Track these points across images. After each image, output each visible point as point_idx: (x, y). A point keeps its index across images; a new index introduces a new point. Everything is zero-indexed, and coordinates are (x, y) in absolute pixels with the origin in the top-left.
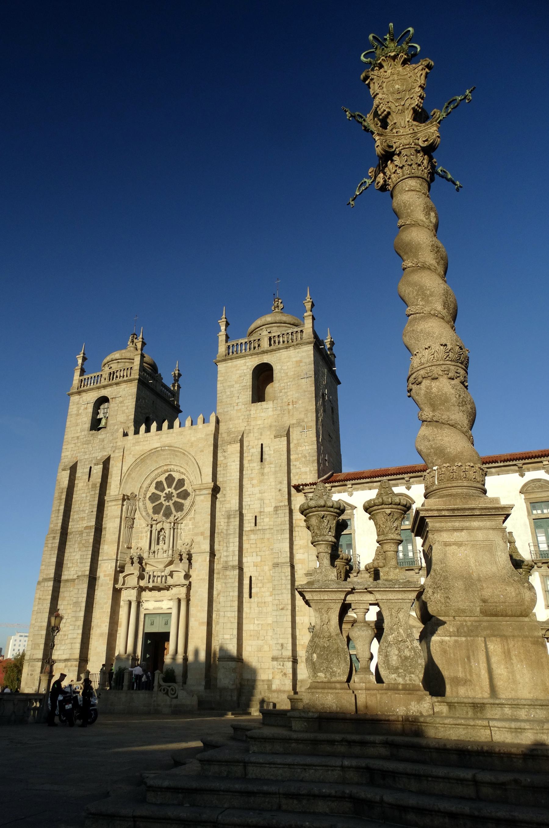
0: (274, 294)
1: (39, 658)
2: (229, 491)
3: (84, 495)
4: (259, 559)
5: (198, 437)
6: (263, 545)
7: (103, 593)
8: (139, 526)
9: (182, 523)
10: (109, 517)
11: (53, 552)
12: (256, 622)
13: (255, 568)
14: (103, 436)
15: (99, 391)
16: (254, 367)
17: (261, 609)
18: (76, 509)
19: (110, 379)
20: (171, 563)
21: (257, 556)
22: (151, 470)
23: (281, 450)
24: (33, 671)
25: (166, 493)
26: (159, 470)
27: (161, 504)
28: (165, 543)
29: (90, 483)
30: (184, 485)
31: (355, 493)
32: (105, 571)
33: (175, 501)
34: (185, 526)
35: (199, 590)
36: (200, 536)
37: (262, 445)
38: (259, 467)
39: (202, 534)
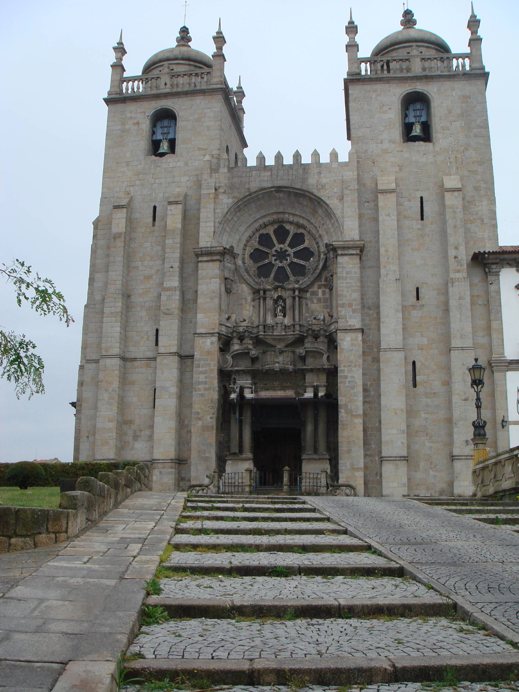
3: (149, 244)
4: (425, 341)
9: (308, 291)
10: (200, 277)
11: (114, 319)
12: (423, 415)
15: (159, 102)
16: (402, 96)
18: (139, 264)
19: (172, 85)
20: (300, 341)
21: (422, 336)
25: (276, 251)
26: (265, 220)
28: (284, 316)
29: (156, 228)
30: (303, 242)
33: (292, 263)
37: (422, 198)
39: (350, 305)
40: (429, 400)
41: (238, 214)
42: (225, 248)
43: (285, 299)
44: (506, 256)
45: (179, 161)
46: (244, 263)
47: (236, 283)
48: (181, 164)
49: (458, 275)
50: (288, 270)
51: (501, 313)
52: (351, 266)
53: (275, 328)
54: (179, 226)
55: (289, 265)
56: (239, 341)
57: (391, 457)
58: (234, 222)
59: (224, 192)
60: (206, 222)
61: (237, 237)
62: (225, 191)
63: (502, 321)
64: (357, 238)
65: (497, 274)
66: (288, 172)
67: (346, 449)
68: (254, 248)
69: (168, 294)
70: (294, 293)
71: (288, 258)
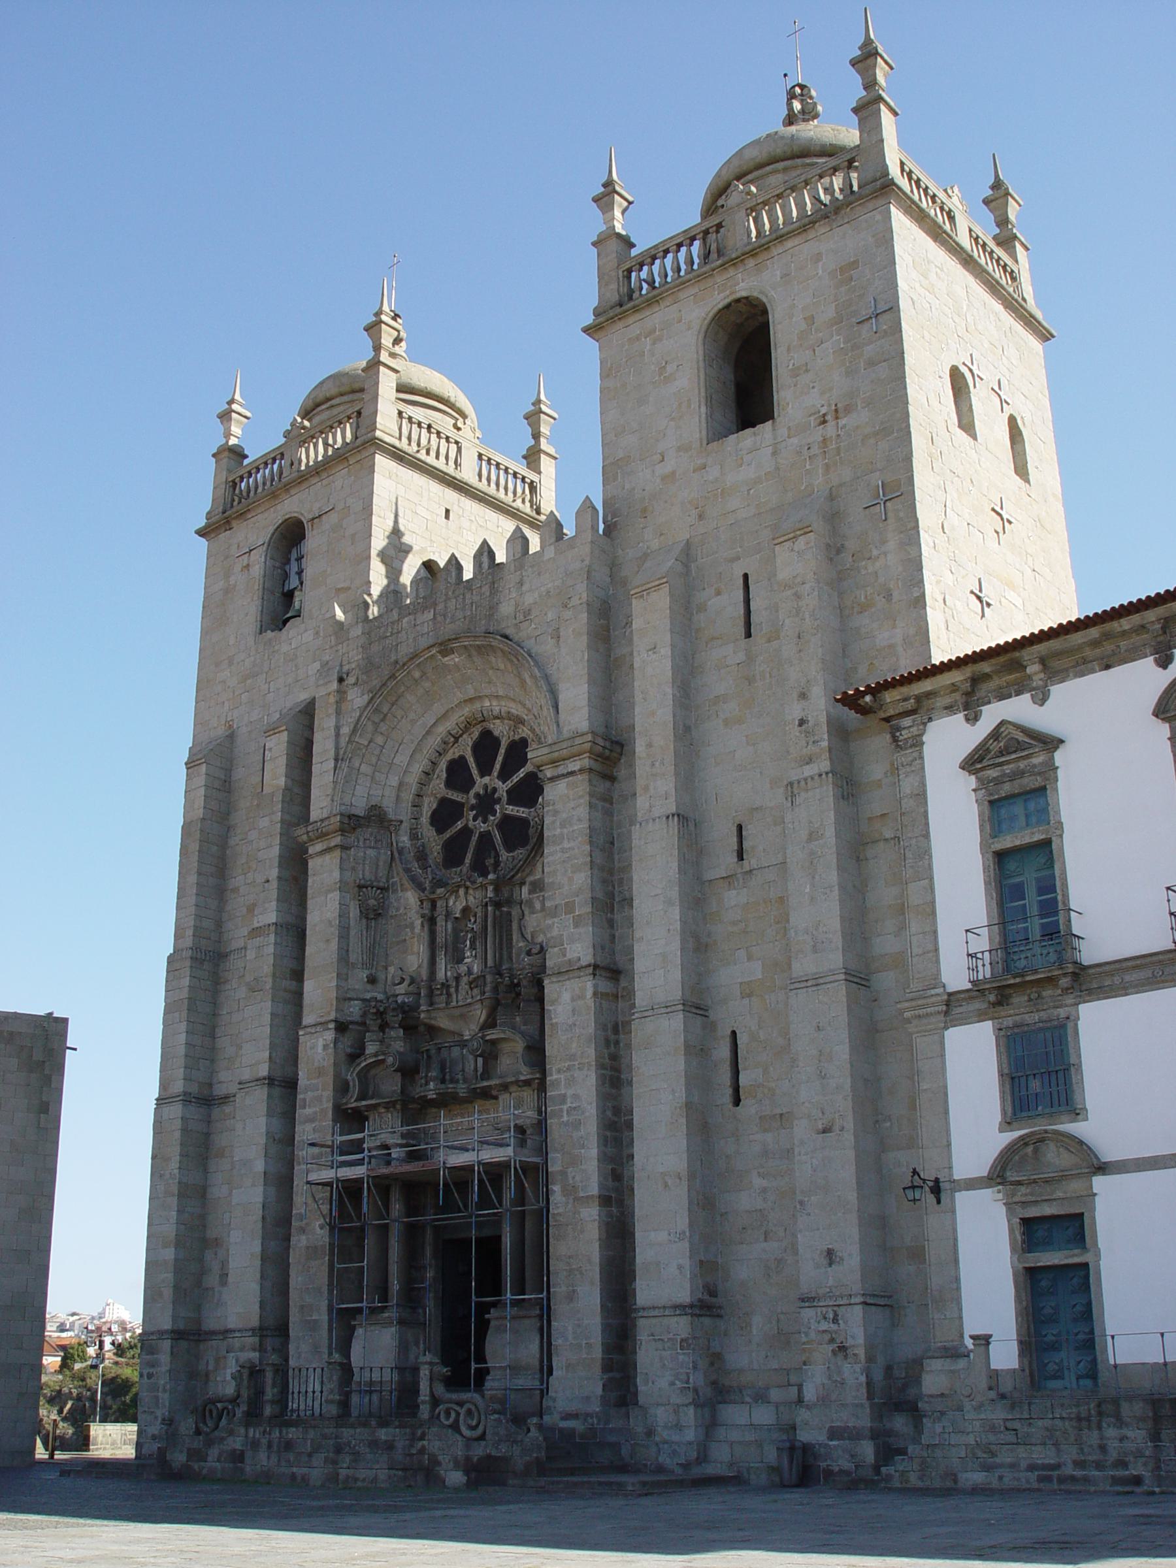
0: (785, 75)
1: (166, 1327)
9: (523, 883)
13: (746, 1001)
15: (279, 507)
21: (750, 958)
23: (799, 580)
24: (153, 1366)
26: (450, 725)
27: (466, 832)
31: (1057, 690)
37: (746, 576)
38: (741, 656)
40: (769, 1137)
41: (383, 728)
44: (926, 685)
45: (306, 631)
46: (414, 836)
47: (395, 891)
48: (308, 636)
49: (809, 770)
50: (497, 837)
51: (931, 857)
52: (572, 804)
53: (452, 990)
54: (282, 781)
58: (378, 749)
59: (355, 684)
61: (394, 781)
62: (357, 678)
63: (931, 879)
64: (584, 726)
65: (917, 743)
66: (464, 599)
67: (564, 1288)
71: (497, 807)
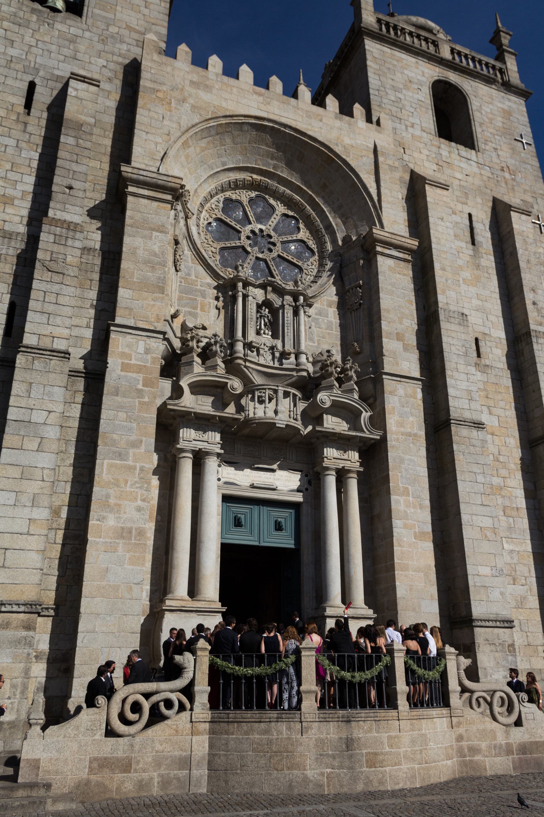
2: (440, 272)
3: (12, 142)
5: (358, 142)
6: (499, 397)
7: (122, 415)
8: (193, 277)
14: (72, 30)
17: (511, 520)
21: (490, 413)
22: (224, 164)
25: (253, 232)
32: (129, 357)
33: (279, 256)
34: (320, 313)
35: (408, 457)
36: (396, 341)
37: (470, 215)
38: (471, 252)
39: (399, 337)
42: (183, 187)
43: (277, 310)
53: (262, 351)
55: (273, 259)
56: (198, 360)
57: (488, 621)
60: (147, 133)
68: (214, 216)
69: (58, 233)
70: (296, 300)
